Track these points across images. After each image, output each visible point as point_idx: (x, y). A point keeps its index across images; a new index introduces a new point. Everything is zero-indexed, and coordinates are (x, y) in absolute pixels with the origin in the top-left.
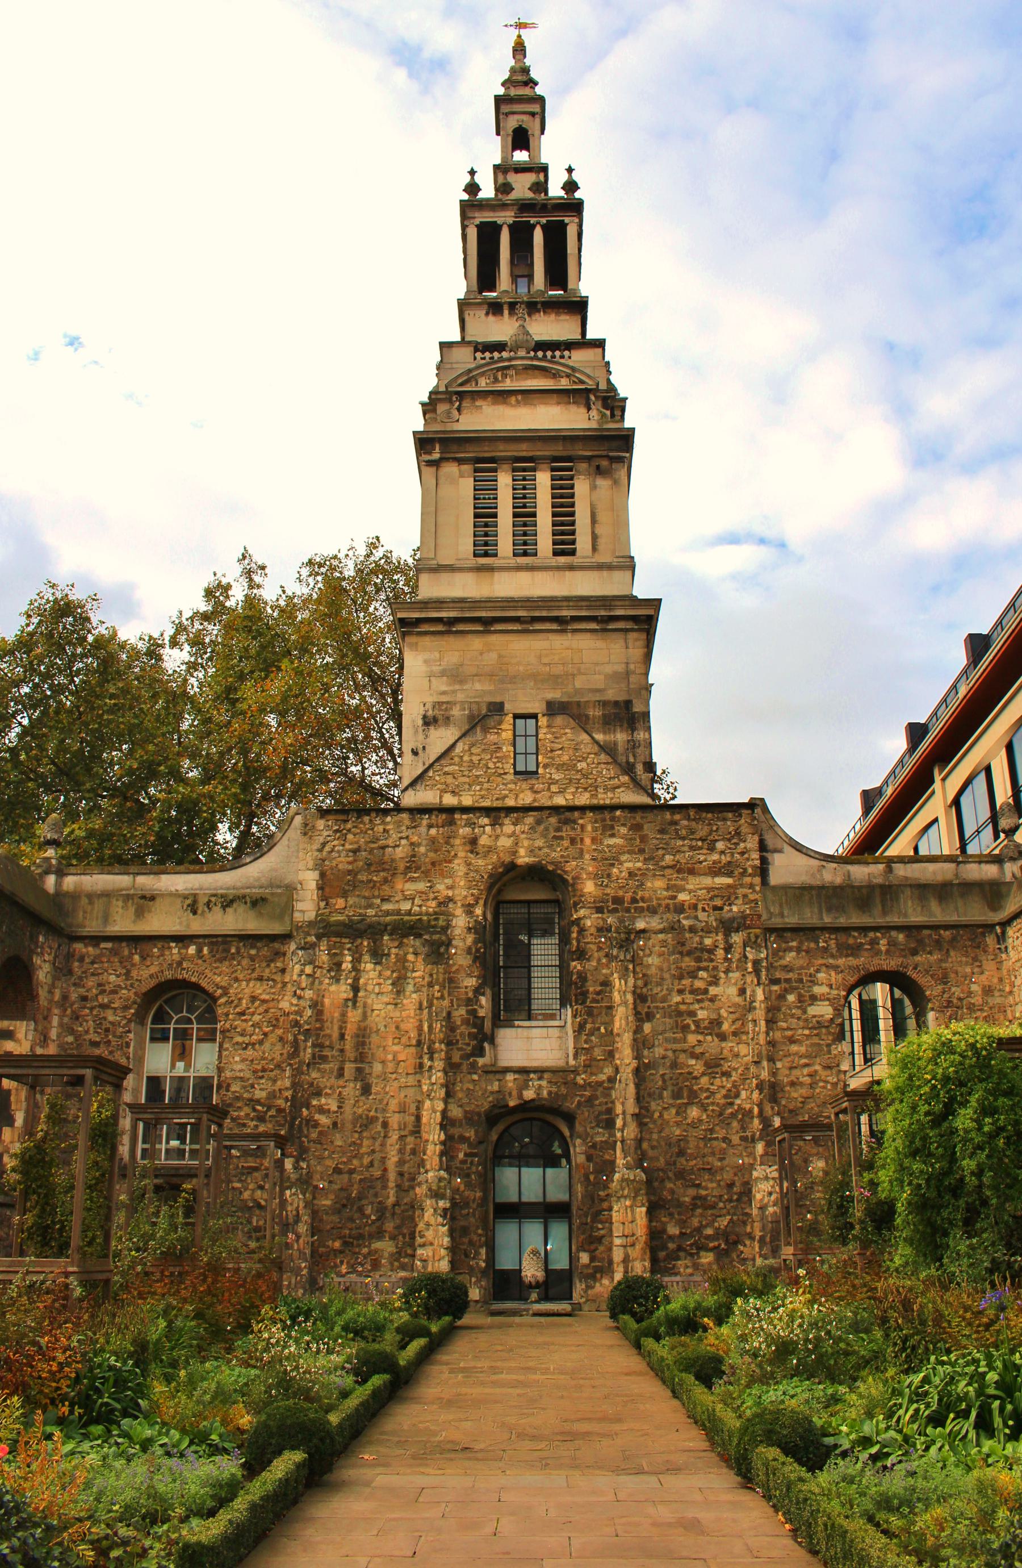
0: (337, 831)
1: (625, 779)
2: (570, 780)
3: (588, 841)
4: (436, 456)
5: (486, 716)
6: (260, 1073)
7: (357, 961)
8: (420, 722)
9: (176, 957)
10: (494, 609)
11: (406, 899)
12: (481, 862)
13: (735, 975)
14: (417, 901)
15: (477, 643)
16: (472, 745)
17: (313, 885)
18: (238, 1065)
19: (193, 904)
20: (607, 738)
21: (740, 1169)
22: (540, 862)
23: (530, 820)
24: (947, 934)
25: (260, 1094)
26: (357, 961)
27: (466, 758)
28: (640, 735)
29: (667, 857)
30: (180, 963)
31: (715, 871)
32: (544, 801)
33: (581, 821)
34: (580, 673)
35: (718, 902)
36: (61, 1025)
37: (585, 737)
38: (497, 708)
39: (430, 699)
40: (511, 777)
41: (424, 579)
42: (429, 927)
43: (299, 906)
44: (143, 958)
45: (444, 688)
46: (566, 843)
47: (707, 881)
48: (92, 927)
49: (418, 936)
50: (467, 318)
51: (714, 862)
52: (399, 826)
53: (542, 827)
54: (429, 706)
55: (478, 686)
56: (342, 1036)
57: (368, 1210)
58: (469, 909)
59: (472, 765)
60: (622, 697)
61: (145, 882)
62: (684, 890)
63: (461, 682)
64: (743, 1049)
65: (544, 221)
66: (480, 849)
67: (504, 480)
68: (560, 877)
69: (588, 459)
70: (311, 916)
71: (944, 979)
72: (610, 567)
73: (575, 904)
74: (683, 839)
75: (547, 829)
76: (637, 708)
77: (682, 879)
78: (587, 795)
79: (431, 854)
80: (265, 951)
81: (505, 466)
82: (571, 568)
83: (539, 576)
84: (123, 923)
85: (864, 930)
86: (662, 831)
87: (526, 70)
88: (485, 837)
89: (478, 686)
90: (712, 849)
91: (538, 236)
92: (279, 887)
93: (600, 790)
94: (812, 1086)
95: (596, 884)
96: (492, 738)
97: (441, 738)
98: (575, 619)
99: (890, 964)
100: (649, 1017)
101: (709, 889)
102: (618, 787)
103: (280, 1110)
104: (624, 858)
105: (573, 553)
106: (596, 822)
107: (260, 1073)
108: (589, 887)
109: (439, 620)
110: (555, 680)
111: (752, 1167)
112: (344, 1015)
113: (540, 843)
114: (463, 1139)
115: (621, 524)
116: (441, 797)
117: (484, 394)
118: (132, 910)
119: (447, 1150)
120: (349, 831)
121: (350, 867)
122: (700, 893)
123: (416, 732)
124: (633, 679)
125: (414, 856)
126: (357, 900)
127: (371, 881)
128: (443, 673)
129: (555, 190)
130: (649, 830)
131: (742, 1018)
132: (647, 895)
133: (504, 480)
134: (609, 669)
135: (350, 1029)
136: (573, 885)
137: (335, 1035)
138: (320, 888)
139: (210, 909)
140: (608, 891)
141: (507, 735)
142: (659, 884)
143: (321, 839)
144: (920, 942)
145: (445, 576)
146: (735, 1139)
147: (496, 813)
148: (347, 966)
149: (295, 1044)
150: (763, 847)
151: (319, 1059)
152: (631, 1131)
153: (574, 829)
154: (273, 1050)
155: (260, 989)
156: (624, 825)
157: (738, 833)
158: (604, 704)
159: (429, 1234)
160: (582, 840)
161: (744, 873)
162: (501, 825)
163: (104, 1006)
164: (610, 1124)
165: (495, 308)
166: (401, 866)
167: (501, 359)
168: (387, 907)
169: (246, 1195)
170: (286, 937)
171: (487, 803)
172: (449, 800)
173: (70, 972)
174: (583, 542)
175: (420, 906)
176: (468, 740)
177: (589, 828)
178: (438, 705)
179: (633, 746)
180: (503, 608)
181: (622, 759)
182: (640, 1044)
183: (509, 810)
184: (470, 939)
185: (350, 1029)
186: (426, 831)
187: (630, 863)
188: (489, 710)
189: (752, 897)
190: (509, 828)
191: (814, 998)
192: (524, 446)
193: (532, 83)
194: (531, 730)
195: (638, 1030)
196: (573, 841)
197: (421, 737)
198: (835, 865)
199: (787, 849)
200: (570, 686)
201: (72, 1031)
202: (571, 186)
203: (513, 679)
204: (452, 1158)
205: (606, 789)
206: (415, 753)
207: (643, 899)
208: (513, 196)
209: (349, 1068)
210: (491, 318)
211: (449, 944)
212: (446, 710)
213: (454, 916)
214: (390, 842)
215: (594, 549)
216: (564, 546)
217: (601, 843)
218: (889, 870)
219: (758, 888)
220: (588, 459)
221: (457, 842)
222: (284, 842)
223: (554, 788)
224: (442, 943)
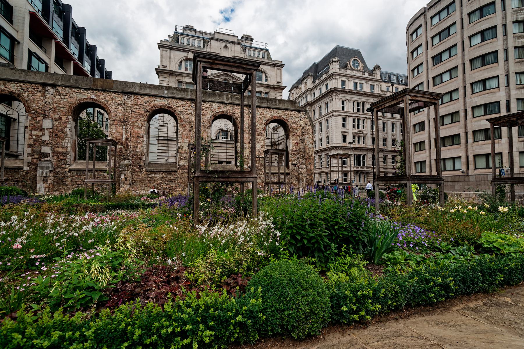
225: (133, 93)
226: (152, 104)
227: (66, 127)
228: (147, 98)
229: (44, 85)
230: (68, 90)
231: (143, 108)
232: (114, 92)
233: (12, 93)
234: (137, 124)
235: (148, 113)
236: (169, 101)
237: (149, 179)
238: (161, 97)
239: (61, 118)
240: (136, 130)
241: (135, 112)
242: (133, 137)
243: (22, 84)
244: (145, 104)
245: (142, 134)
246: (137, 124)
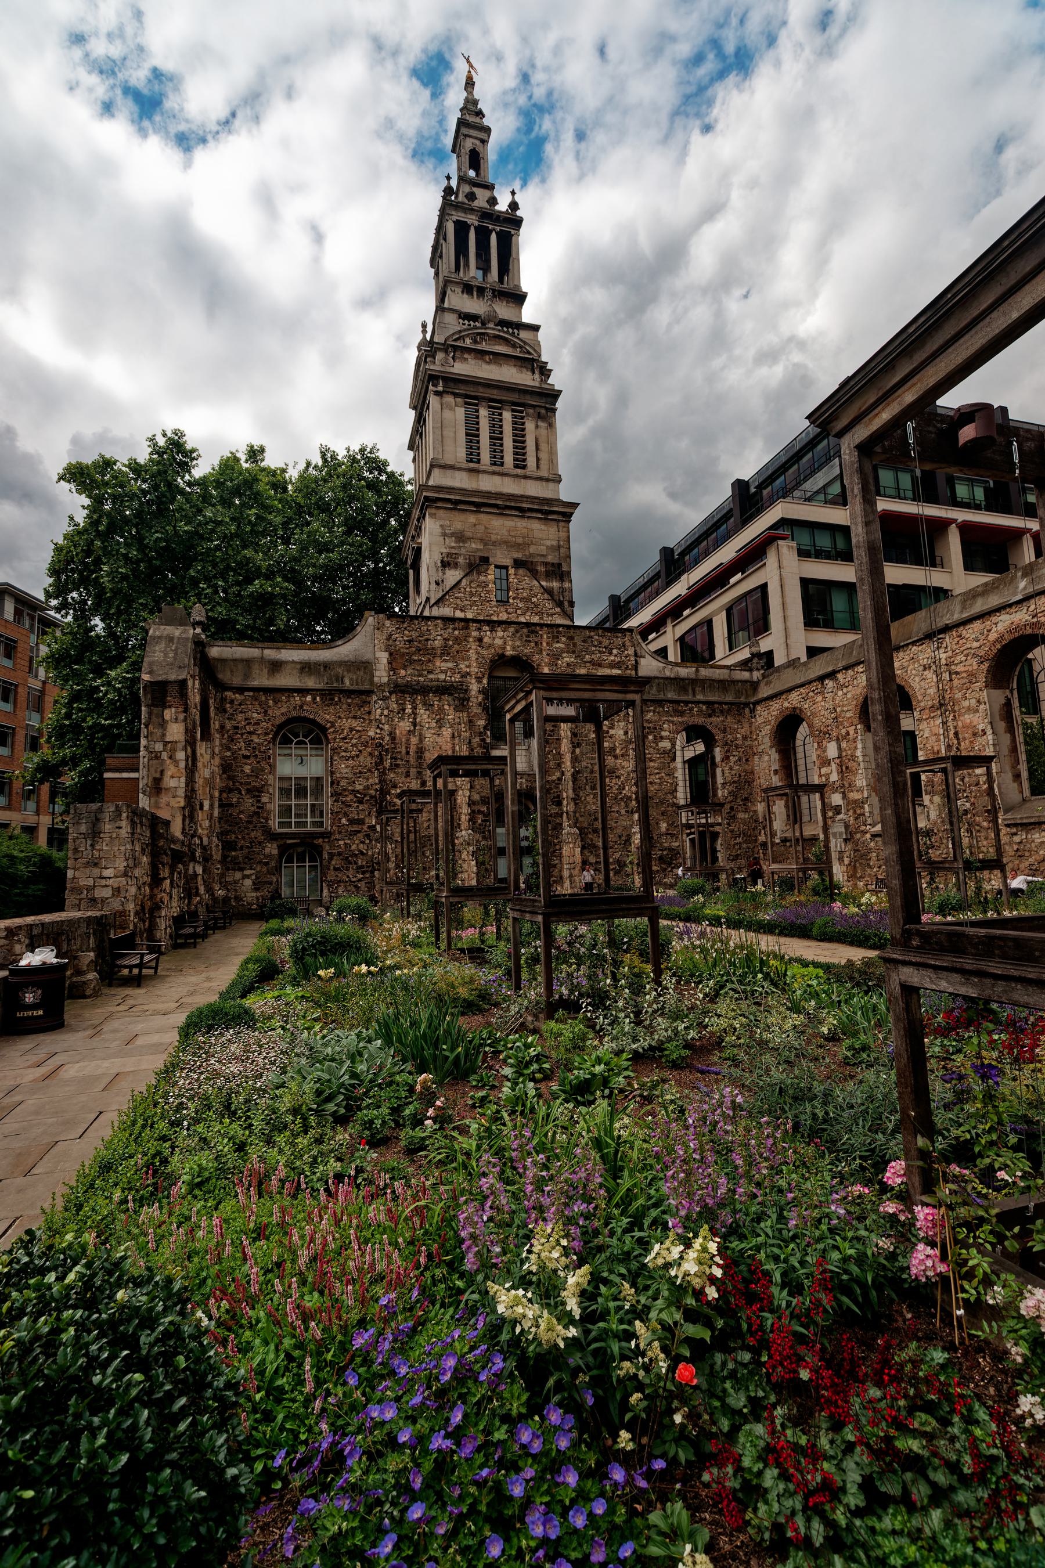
1: (558, 610)
4: (440, 389)
6: (359, 774)
7: (414, 708)
9: (299, 703)
10: (483, 497)
13: (622, 724)
15: (472, 518)
17: (385, 661)
18: (343, 768)
19: (306, 668)
21: (625, 828)
23: (512, 630)
24: (725, 707)
25: (358, 787)
26: (414, 708)
28: (566, 585)
30: (301, 706)
31: (612, 665)
32: (513, 618)
36: (221, 745)
39: (445, 551)
41: (436, 472)
42: (456, 689)
43: (377, 673)
44: (276, 702)
48: (237, 681)
49: (450, 694)
50: (449, 292)
55: (473, 546)
56: (408, 753)
57: (428, 853)
58: (479, 680)
59: (472, 594)
60: (556, 561)
61: (270, 654)
63: (464, 542)
64: (625, 764)
65: (498, 229)
69: (534, 407)
70: (385, 680)
71: (724, 731)
72: (547, 480)
76: (565, 568)
80: (357, 701)
82: (525, 477)
83: (506, 479)
84: (262, 680)
85: (687, 703)
86: (584, 641)
87: (475, 102)
89: (473, 546)
90: (611, 653)
91: (493, 238)
94: (660, 784)
96: (482, 578)
99: (699, 721)
100: (579, 745)
103: (372, 797)
105: (524, 467)
107: (359, 774)
110: (518, 546)
111: (631, 826)
112: (408, 740)
113: (518, 643)
114: (479, 812)
115: (553, 452)
117: (469, 350)
118: (265, 671)
119: (472, 819)
124: (562, 550)
129: (502, 206)
130: (578, 640)
131: (626, 747)
133: (483, 413)
134: (548, 543)
135: (413, 749)
137: (404, 751)
138: (389, 663)
144: (714, 711)
145: (449, 472)
146: (623, 812)
147: (493, 625)
148: (408, 711)
149: (381, 757)
150: (636, 655)
151: (395, 766)
152: (571, 807)
154: (364, 760)
155: (354, 724)
158: (546, 564)
159: (465, 866)
163: (250, 733)
164: (559, 804)
165: (468, 288)
166: (439, 652)
167: (475, 328)
168: (431, 676)
169: (354, 847)
170: (369, 693)
172: (459, 614)
173: (225, 711)
174: (531, 461)
176: (469, 578)
178: (449, 555)
179: (562, 590)
180: (489, 498)
182: (575, 760)
183: (500, 623)
184: (480, 698)
185: (413, 749)
187: (567, 658)
190: (500, 634)
191: (662, 738)
192: (495, 392)
193: (480, 114)
194: (504, 576)
195: (573, 752)
196: (536, 644)
201: (229, 749)
202: (514, 206)
203: (494, 543)
204: (474, 823)
205: (549, 615)
206: (437, 583)
208: (476, 204)
209: (413, 771)
210: (465, 296)
211: (468, 700)
215: (538, 467)
216: (520, 462)
220: (534, 407)
222: (363, 633)
224: (464, 699)
225: (947, 629)
226: (993, 636)
227: (856, 748)
228: (977, 625)
229: (821, 679)
230: (850, 672)
231: (975, 656)
232: (914, 643)
233: (794, 708)
234: (966, 704)
235: (985, 666)
236: (1032, 607)
237: (1015, 847)
238: (1010, 606)
239: (848, 734)
240: (967, 718)
241: (957, 673)
242: (964, 739)
243: (802, 690)
244: (976, 644)
245: (981, 727)
246: (966, 704)
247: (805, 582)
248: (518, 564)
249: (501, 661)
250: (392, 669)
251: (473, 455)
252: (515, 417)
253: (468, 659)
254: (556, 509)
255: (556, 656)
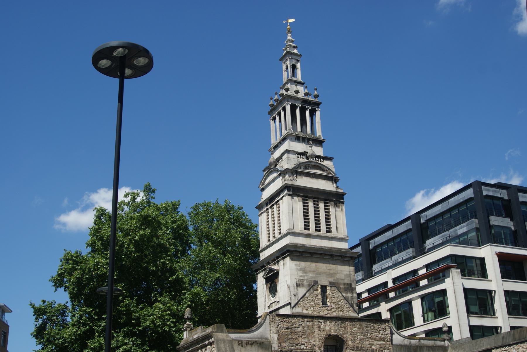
0: (282, 321)
1: (351, 308)
2: (337, 307)
3: (349, 329)
4: (291, 193)
5: (314, 285)
8: (295, 285)
11: (302, 344)
12: (322, 334)
14: (305, 345)
16: (310, 294)
17: (276, 339)
20: (346, 295)
22: (337, 334)
27: (309, 298)
29: (368, 335)
33: (347, 323)
34: (338, 273)
35: (382, 349)
37: (340, 294)
38: (316, 283)
39: (298, 278)
40: (321, 305)
43: (273, 345)
45: (301, 274)
46: (343, 329)
47: (379, 343)
51: (380, 337)
52: (299, 321)
53: (337, 324)
54: (297, 280)
55: (311, 275)
59: (311, 301)
60: (349, 282)
62: (373, 345)
63: (306, 273)
66: (322, 330)
67: (311, 204)
68: (342, 339)
70: (276, 348)
73: (347, 348)
74: (372, 329)
75: (338, 324)
77: (373, 342)
78: (342, 313)
79: (308, 330)
81: (311, 200)
86: (366, 327)
88: (322, 326)
89: (311, 275)
90: (379, 333)
91: (308, 113)
92: (264, 338)
93: (345, 311)
95: (352, 342)
96: (315, 292)
97: (302, 291)
98: (336, 256)
101: (380, 345)
102: (350, 311)
104: (358, 334)
106: (350, 323)
108: (350, 343)
109: (299, 252)
110: (331, 275)
116: (303, 310)
120: (285, 321)
121: (286, 333)
122: (377, 346)
123: (294, 288)
124: (352, 276)
125: (304, 331)
126: (289, 344)
127: (292, 338)
128: (301, 269)
132: (364, 346)
133: (311, 204)
134: (345, 273)
136: (346, 342)
138: (278, 340)
139: (247, 345)
140: (355, 344)
141: (319, 291)
142: (367, 343)
143: (277, 324)
153: (345, 324)
156: (358, 324)
157: (385, 329)
158: (344, 284)
160: (347, 328)
161: (387, 341)
162: (326, 322)
165: (298, 138)
166: (301, 333)
168: (297, 347)
171: (315, 314)
172: (305, 312)
174: (333, 229)
175: (306, 347)
176: (308, 292)
177: (349, 324)
178: (300, 280)
179: (353, 298)
181: (350, 302)
186: (306, 323)
187: (360, 336)
188: (314, 283)
189: (390, 348)
196: (345, 328)
197: (296, 290)
198: (407, 339)
199: (396, 333)
200: (335, 277)
203: (320, 274)
206: (295, 295)
207: (363, 347)
212: (302, 282)
213: (316, 350)
214: (297, 326)
216: (329, 231)
217: (352, 330)
218: (420, 341)
219: (391, 345)
221: (315, 327)
223: (333, 310)
247: (467, 291)
248: (332, 284)
249: (329, 337)
250: (280, 343)
251: (307, 227)
252: (325, 206)
253: (314, 337)
254: (348, 255)
255: (355, 335)
